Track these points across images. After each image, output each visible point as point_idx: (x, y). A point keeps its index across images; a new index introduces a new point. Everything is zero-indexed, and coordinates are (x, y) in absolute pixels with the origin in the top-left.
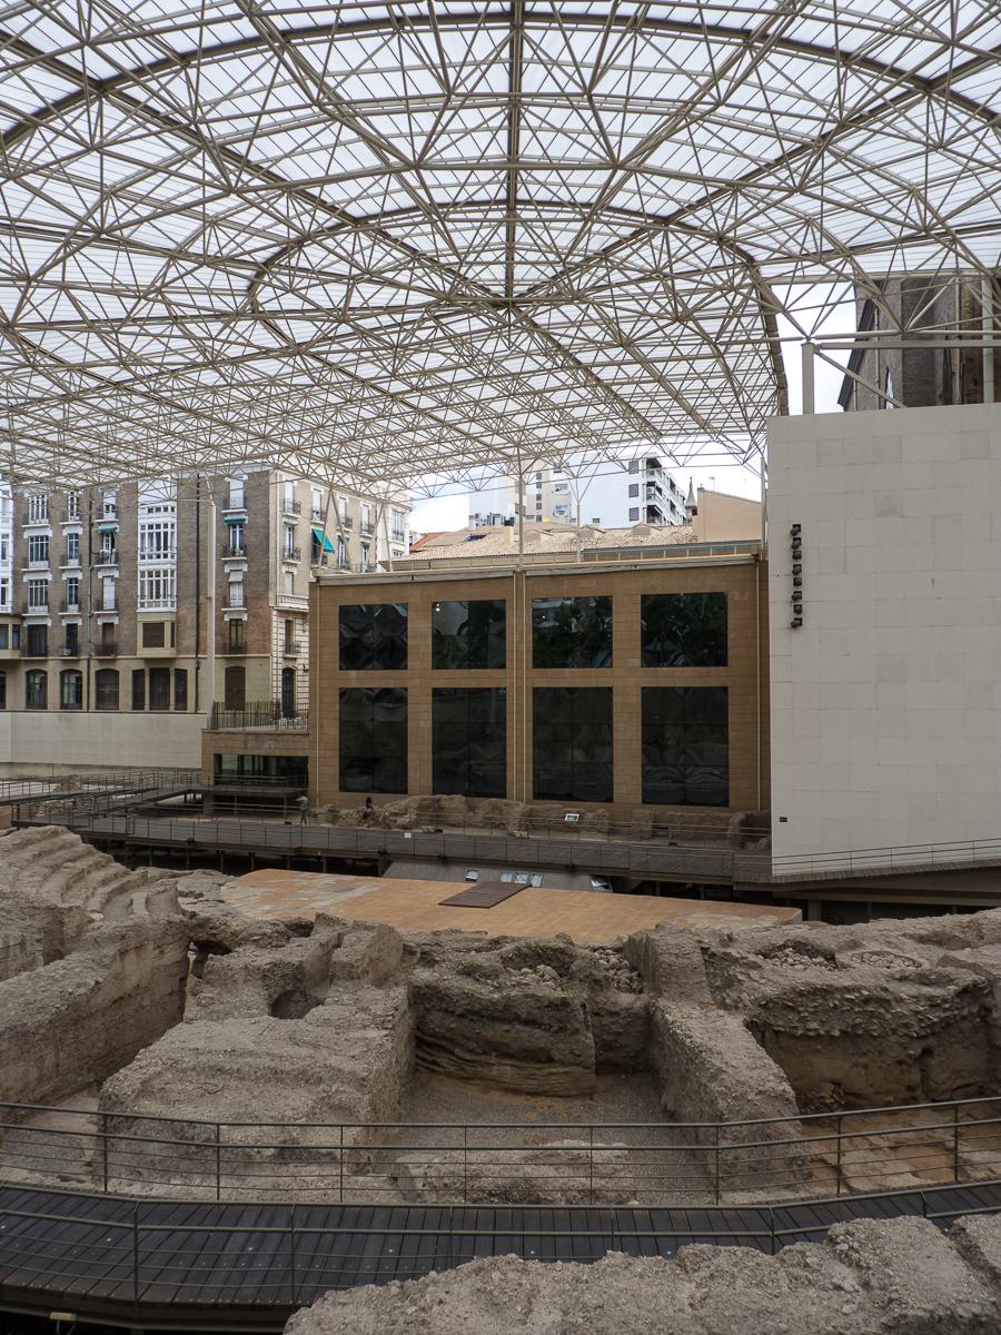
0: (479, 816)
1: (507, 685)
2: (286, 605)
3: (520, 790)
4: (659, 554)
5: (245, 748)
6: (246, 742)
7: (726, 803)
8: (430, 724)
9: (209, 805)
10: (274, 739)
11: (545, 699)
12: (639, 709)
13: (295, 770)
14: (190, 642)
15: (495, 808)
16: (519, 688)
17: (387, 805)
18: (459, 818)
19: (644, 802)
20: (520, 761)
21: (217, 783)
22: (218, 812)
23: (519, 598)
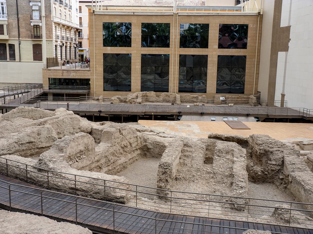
0: (161, 98)
1: (170, 53)
2: (56, 20)
3: (174, 89)
4: (193, 10)
5: (63, 75)
6: (63, 73)
7: (243, 93)
8: (140, 67)
9: (50, 97)
10: (74, 71)
11: (183, 60)
12: (216, 63)
13: (85, 83)
14: (15, 33)
15: (167, 96)
16: (175, 55)
17: (130, 96)
18: (154, 99)
19: (217, 93)
20: (174, 80)
21: (50, 89)
22: (54, 100)
23: (176, 23)
